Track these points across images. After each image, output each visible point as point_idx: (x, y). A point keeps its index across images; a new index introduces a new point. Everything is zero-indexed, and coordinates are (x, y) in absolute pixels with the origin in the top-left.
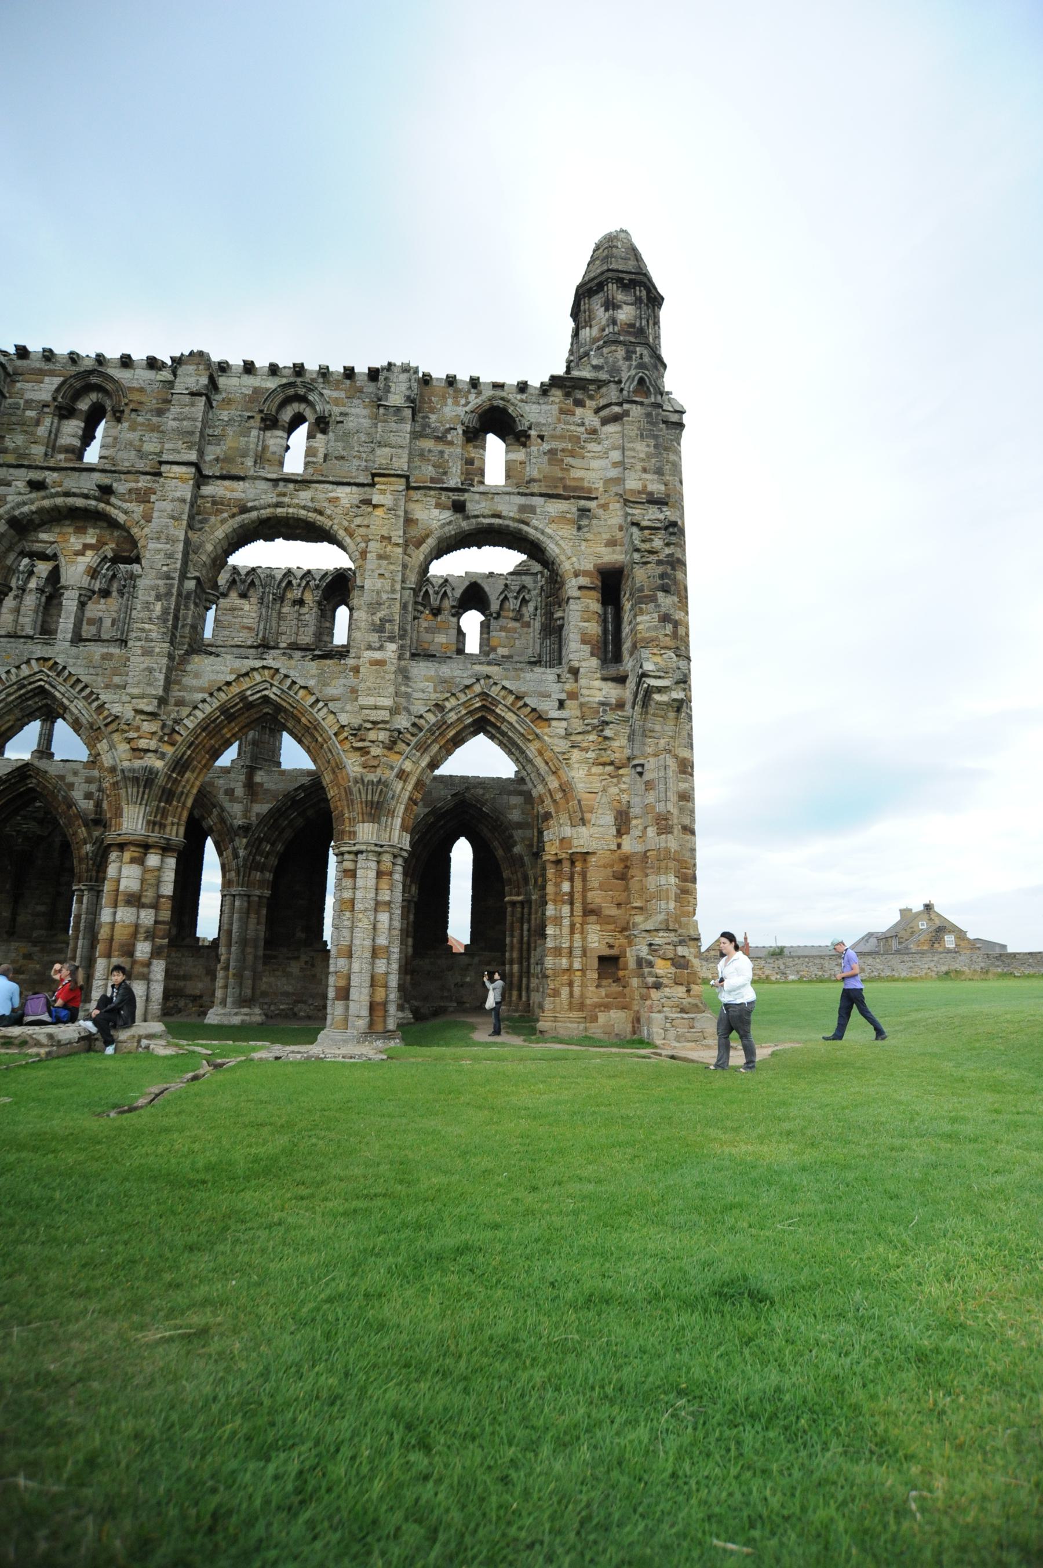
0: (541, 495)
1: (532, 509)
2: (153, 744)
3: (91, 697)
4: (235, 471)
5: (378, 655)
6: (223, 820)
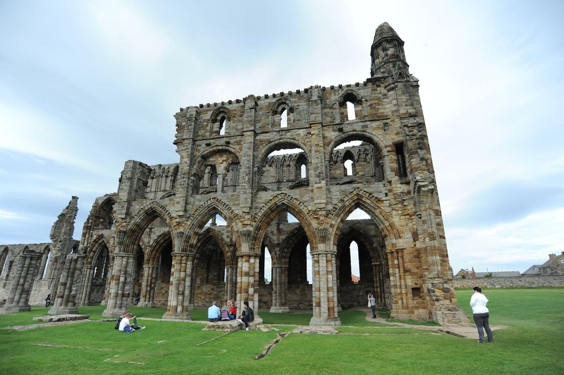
0: (369, 121)
1: (367, 126)
2: (249, 222)
3: (229, 209)
4: (266, 130)
5: (319, 185)
6: (271, 242)
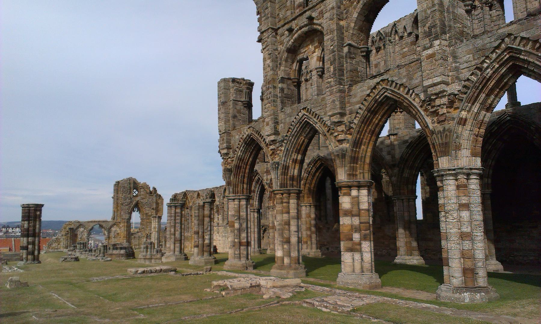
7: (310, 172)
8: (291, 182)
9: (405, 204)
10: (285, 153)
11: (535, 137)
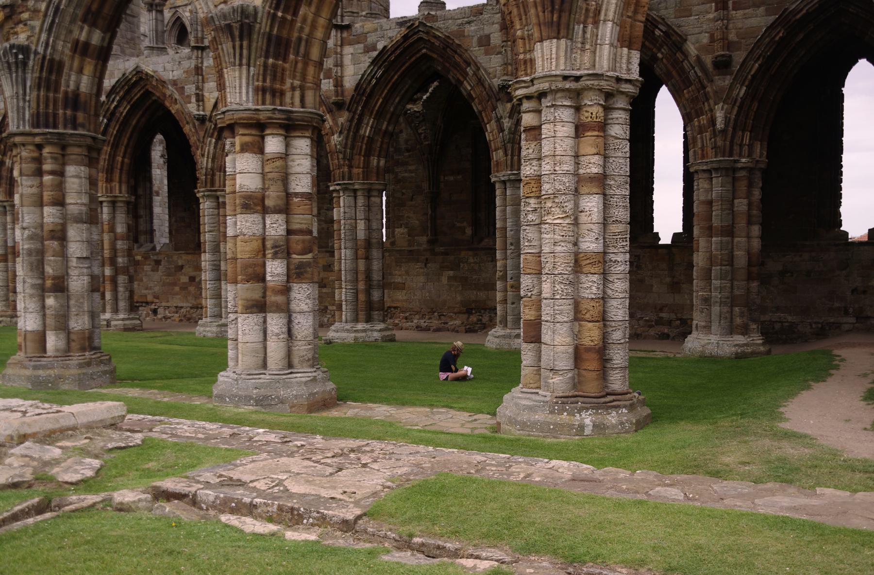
6: (480, 82)
7: (113, 114)
8: (69, 112)
9: (361, 201)
10: (49, 20)
11: (660, 55)
